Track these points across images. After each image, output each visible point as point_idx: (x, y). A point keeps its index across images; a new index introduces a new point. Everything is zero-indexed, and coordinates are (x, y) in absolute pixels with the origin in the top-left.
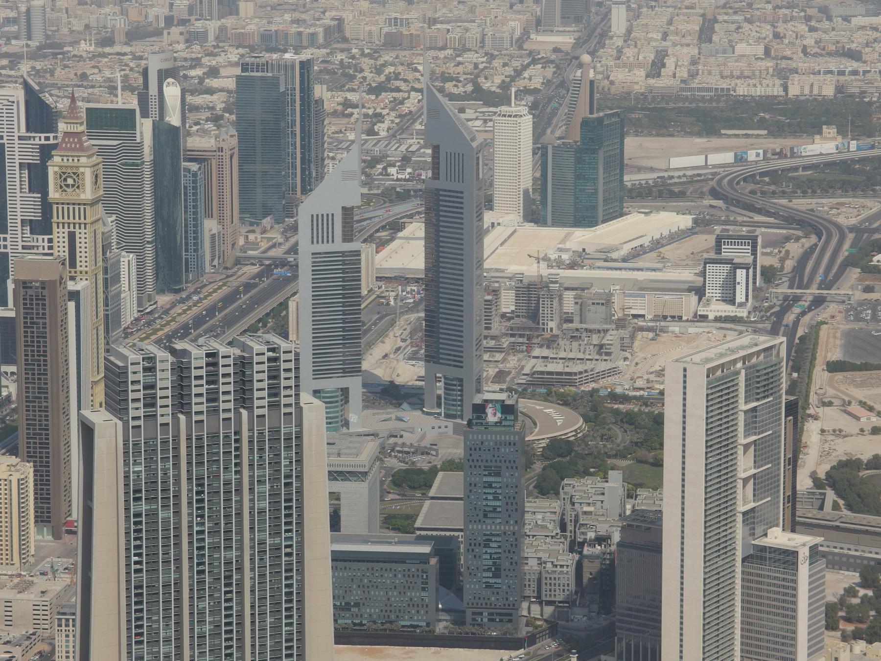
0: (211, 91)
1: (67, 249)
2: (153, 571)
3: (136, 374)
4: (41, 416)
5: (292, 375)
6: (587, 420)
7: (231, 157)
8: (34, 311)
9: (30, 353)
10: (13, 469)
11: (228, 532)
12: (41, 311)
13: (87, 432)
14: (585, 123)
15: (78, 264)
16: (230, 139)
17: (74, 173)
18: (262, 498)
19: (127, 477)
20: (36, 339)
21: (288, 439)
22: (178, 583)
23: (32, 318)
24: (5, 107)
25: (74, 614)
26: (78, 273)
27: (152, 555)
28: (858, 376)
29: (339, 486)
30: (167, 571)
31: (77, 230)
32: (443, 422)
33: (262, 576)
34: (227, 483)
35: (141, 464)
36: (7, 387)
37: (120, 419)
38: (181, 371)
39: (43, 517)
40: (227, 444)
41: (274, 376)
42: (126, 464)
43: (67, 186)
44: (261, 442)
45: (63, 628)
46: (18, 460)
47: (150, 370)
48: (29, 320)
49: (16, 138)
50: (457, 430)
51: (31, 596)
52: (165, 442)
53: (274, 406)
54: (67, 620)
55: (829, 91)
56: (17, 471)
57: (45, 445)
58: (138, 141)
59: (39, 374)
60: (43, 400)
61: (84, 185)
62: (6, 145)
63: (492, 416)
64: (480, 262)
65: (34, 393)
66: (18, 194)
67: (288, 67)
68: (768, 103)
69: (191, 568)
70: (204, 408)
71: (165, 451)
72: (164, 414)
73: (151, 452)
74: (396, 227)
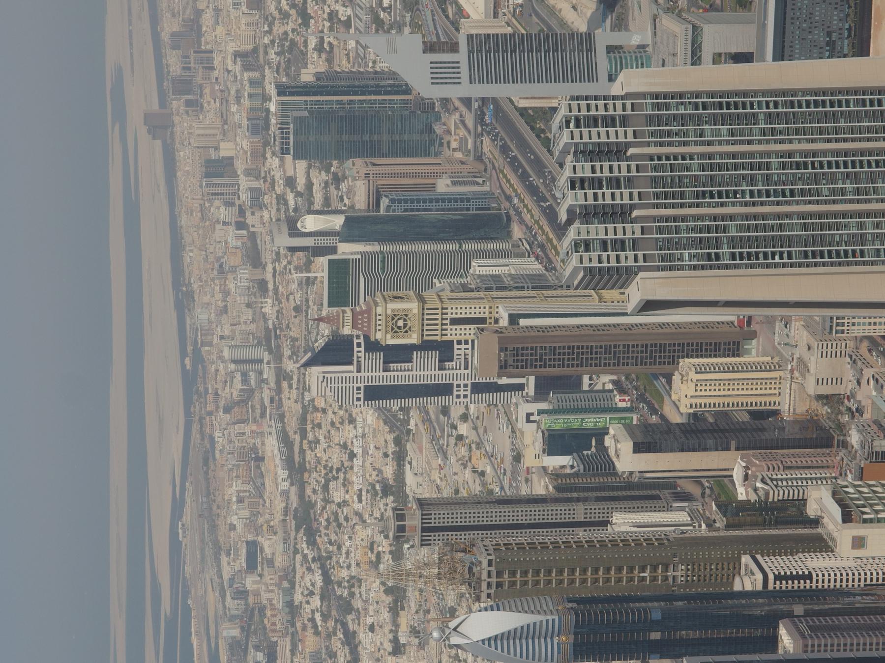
0: (309, 185)
1: (468, 327)
2: (790, 241)
3: (592, 258)
4: (633, 352)
5: (593, 103)
7: (374, 165)
8: (529, 358)
10: (685, 378)
11: (752, 166)
12: (529, 352)
13: (649, 306)
15: (482, 315)
16: (356, 166)
17: (393, 319)
18: (718, 133)
19: (695, 268)
20: (557, 357)
21: (658, 107)
22: (803, 216)
24: (329, 385)
25: (832, 318)
26: (490, 315)
27: (773, 242)
29: (707, 54)
30: (791, 227)
31: (449, 316)
33: (797, 131)
34: (702, 168)
35: (681, 254)
36: (604, 384)
37: (637, 274)
38: (588, 214)
39: (735, 349)
40: (663, 168)
41: (594, 122)
42: (681, 268)
43: (405, 325)
44: (661, 134)
45: (845, 328)
46: (676, 373)
48: (538, 363)
49: (359, 375)
51: (813, 360)
52: (660, 230)
53: (625, 122)
54: (838, 324)
56: (687, 374)
57: (662, 348)
58: (360, 257)
59: (591, 354)
60: (617, 350)
61: (404, 310)
62: (366, 384)
67: (284, 108)
69: (788, 203)
70: (626, 192)
71: (669, 230)
72: (632, 231)
73: (669, 244)
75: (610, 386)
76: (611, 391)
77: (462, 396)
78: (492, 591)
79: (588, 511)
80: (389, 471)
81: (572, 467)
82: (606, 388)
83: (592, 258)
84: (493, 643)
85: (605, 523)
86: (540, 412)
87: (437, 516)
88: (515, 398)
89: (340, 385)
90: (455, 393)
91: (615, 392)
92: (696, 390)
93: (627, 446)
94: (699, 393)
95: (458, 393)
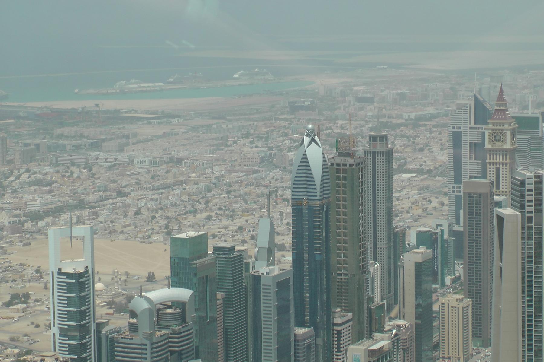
1: (495, 175)
8: (474, 211)
9: (471, 225)
12: (478, 211)
15: (501, 187)
17: (501, 133)
20: (475, 250)
23: (473, 215)
26: (501, 192)
37: (520, 212)
48: (471, 217)
49: (468, 128)
58: (540, 136)
59: (476, 249)
60: (478, 264)
61: (506, 140)
62: (462, 133)
65: (473, 260)
66: (468, 161)
75: (457, 275)
76: (454, 274)
77: (454, 189)
78: (335, 166)
79: (382, 250)
80: (411, 166)
81: (409, 245)
82: (456, 272)
83: (530, 185)
84: (304, 160)
85: (375, 259)
86: (442, 231)
87: (382, 161)
89: (462, 115)
90: (455, 185)
91: (453, 277)
92: (452, 307)
94: (450, 308)
95: (455, 187)
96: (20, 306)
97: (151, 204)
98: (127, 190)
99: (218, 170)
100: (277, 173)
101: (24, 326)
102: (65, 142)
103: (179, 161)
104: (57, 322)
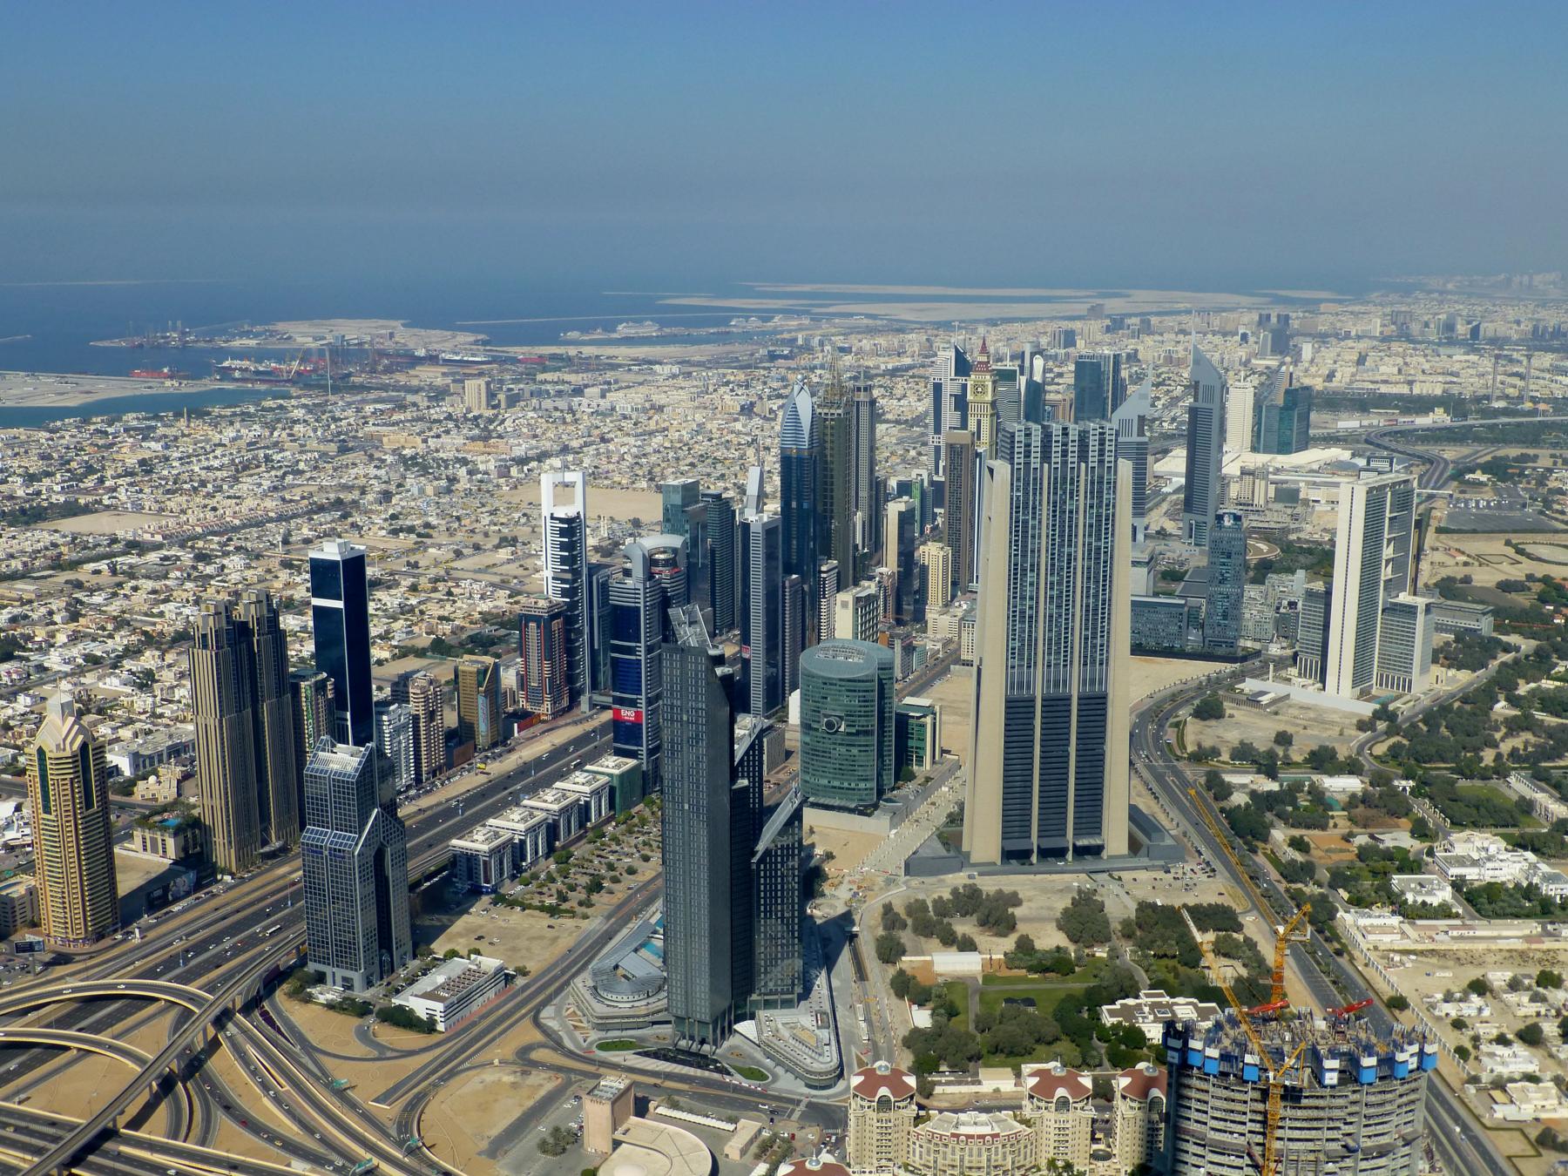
0: (1058, 384)
2: (1024, 556)
3: (1020, 437)
6: (1282, 551)
14: (1287, 392)
16: (1072, 395)
18: (1091, 518)
21: (1109, 483)
28: (1455, 536)
30: (1032, 557)
32: (1192, 547)
38: (1047, 436)
47: (1028, 435)
50: (1202, 553)
53: (1101, 462)
55: (1438, 391)
63: (1228, 522)
64: (1220, 469)
67: (1107, 358)
68: (1400, 397)
72: (1035, 461)
74: (1166, 452)
80: (889, 416)
83: (1020, 437)
88: (932, 467)
93: (902, 508)
96: (510, 549)
97: (634, 450)
98: (611, 435)
99: (699, 417)
100: (757, 421)
101: (512, 569)
102: (548, 387)
103: (661, 409)
104: (550, 566)
